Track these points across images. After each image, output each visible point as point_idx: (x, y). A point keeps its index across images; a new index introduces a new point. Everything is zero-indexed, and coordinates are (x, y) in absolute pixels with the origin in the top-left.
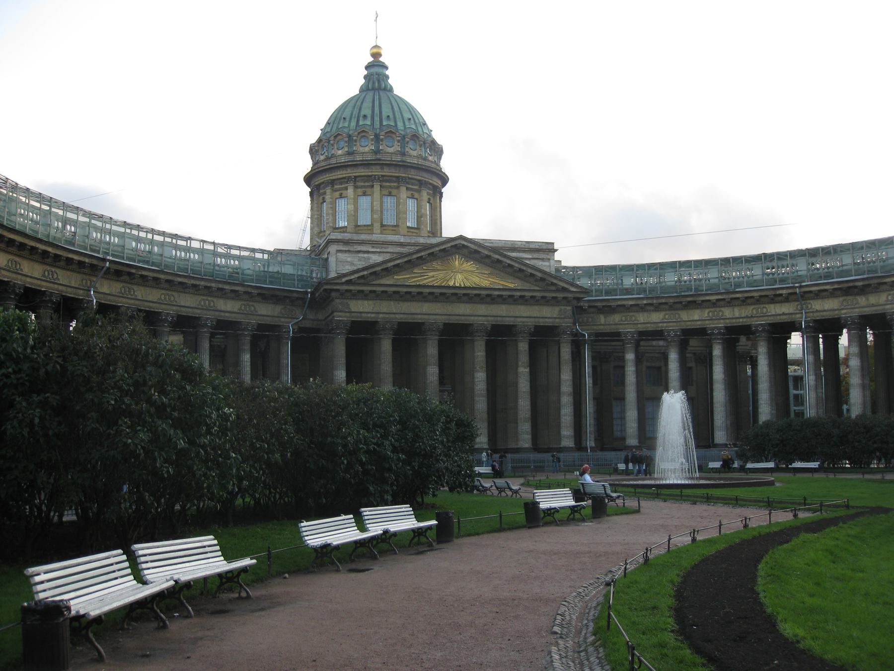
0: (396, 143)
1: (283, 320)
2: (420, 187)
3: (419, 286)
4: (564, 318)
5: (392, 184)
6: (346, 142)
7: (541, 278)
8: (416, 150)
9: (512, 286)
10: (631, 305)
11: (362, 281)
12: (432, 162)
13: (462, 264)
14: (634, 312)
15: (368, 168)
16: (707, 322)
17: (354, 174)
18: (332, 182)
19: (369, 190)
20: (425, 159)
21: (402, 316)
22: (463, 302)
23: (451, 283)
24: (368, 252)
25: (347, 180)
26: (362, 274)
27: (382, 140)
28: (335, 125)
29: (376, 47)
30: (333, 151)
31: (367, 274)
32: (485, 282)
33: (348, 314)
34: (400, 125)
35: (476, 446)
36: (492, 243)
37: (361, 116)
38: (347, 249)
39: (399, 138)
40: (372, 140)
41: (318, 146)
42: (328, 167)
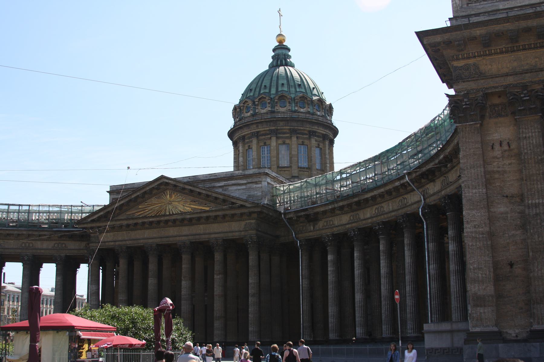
4: (248, 231)
5: (267, 137)
8: (286, 106)
9: (207, 209)
12: (301, 112)
15: (249, 128)
16: (374, 219)
17: (242, 135)
20: (295, 111)
21: (130, 242)
26: (100, 214)
27: (258, 105)
31: (103, 214)
32: (188, 209)
34: (273, 91)
36: (216, 176)
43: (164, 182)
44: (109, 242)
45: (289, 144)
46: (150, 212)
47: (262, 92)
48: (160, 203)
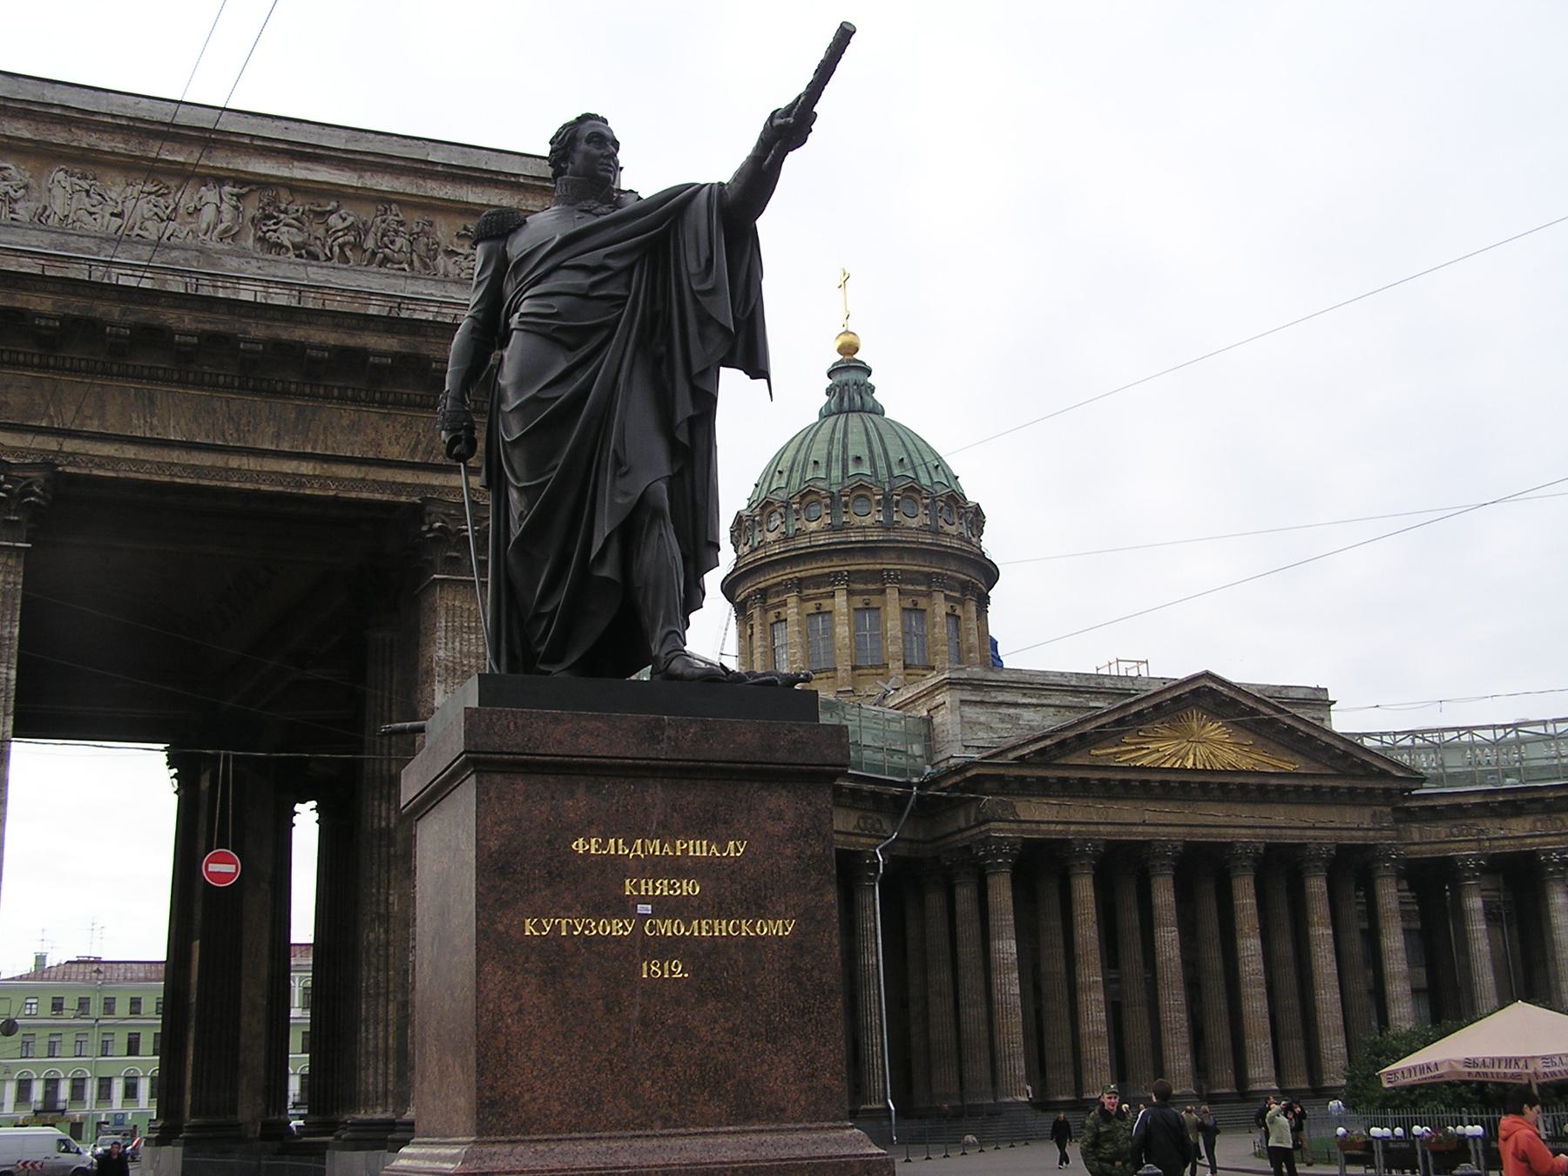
0: (921, 509)
1: (863, 840)
2: (964, 595)
3: (1142, 768)
5: (918, 588)
6: (827, 506)
7: (1344, 751)
8: (953, 524)
9: (1290, 768)
10: (1475, 805)
11: (1038, 759)
13: (1204, 726)
14: (1476, 817)
15: (874, 557)
17: (847, 568)
18: (800, 584)
19: (875, 601)
21: (1109, 828)
22: (1213, 801)
23: (1189, 765)
24: (1016, 705)
25: (832, 579)
26: (1041, 745)
28: (796, 476)
29: (847, 332)
30: (799, 522)
31: (1049, 746)
32: (1245, 764)
33: (1014, 826)
34: (925, 480)
35: (1257, 1087)
37: (850, 458)
38: (978, 699)
39: (928, 501)
40: (878, 503)
41: (761, 515)
42: (793, 553)
43: (1204, 686)
44: (1049, 822)
45: (959, 617)
46: (1156, 756)
47: (897, 472)
48: (1177, 738)
